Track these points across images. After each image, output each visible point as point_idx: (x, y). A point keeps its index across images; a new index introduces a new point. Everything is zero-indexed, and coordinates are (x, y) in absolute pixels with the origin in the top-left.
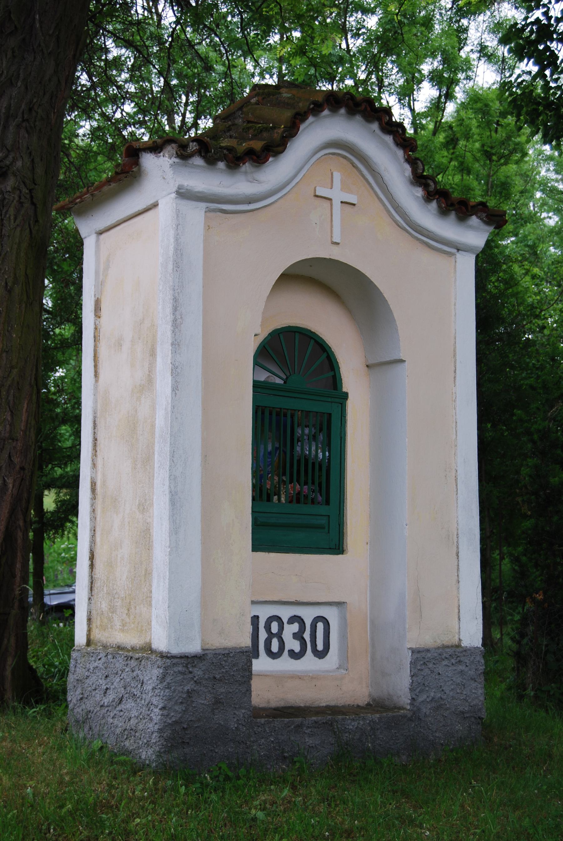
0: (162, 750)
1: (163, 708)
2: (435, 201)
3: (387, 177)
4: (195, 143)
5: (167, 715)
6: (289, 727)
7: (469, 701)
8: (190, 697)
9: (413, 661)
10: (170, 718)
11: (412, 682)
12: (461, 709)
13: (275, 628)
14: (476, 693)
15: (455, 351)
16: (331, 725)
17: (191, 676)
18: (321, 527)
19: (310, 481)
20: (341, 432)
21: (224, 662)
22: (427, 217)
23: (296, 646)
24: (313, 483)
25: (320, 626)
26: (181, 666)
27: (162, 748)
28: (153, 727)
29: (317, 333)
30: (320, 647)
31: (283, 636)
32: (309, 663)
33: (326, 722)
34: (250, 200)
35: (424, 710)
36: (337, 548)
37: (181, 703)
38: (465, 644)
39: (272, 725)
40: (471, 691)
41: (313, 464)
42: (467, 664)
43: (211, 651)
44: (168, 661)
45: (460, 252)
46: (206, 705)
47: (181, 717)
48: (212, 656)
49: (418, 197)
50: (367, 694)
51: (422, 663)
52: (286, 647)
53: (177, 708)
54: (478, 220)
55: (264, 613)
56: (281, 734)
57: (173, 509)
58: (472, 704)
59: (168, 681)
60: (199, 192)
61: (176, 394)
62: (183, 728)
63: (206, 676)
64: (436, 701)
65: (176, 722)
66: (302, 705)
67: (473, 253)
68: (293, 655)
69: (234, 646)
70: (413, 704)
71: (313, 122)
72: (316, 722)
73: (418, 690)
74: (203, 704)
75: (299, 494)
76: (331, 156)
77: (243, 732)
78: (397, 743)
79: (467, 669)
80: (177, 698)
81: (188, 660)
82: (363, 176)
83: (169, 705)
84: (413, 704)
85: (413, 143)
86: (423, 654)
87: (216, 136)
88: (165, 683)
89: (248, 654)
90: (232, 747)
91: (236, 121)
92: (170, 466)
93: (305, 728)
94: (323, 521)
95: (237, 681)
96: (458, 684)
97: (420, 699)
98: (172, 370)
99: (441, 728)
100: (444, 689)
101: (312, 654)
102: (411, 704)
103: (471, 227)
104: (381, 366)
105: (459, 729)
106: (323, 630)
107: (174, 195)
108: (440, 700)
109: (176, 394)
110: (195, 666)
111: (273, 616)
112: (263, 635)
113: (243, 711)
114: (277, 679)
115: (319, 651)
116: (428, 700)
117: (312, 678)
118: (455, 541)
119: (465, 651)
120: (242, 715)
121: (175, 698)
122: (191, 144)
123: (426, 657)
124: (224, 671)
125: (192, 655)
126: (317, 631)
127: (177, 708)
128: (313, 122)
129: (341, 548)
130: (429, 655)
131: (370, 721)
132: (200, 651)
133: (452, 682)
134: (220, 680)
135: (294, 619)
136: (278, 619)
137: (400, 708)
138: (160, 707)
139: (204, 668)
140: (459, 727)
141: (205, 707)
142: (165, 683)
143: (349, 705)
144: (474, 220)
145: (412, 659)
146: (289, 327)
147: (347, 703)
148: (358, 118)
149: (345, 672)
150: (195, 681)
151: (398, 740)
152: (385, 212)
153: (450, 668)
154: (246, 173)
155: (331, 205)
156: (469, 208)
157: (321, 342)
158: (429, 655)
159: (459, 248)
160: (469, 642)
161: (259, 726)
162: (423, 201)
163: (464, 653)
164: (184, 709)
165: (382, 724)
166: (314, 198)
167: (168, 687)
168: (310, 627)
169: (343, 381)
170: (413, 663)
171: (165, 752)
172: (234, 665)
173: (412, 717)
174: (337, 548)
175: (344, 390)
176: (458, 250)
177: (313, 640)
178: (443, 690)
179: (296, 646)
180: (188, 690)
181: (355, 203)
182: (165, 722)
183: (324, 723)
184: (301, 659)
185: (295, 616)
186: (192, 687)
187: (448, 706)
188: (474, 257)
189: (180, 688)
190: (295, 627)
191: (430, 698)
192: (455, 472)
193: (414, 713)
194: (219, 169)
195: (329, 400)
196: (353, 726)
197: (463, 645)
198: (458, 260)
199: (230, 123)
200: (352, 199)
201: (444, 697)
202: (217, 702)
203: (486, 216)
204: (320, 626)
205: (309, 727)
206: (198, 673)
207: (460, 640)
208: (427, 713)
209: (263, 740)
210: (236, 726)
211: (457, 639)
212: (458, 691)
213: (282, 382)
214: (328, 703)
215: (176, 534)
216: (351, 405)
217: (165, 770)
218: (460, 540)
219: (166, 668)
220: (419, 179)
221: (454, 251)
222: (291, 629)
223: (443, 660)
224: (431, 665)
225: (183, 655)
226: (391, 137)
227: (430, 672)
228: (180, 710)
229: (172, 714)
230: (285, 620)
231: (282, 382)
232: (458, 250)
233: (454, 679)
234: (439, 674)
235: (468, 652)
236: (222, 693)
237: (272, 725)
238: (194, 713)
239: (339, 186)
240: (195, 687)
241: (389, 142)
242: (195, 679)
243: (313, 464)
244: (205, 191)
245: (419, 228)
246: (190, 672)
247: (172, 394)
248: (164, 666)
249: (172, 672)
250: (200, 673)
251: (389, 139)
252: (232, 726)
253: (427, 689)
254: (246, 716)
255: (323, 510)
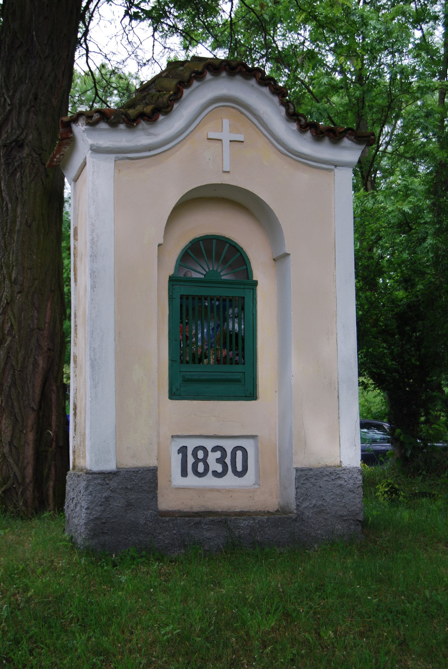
0: (87, 538)
1: (87, 509)
2: (309, 132)
3: (265, 118)
4: (97, 114)
5: (90, 514)
6: (189, 523)
7: (348, 507)
8: (108, 501)
9: (297, 477)
10: (93, 516)
11: (297, 492)
12: (340, 513)
13: (201, 455)
14: (356, 501)
15: (335, 243)
16: (226, 522)
17: (108, 486)
18: (238, 381)
19: (234, 347)
20: (253, 310)
21: (134, 477)
22: (304, 145)
23: (219, 468)
24: (237, 349)
25: (239, 454)
26: (100, 479)
27: (87, 536)
28: (82, 522)
29: (231, 238)
30: (239, 468)
31: (207, 461)
32: (230, 480)
33: (221, 521)
34: (149, 148)
35: (307, 514)
36: (251, 394)
37: (101, 505)
38: (344, 464)
39: (175, 522)
40: (349, 500)
41: (231, 336)
42: (346, 480)
43: (124, 470)
44: (90, 476)
45: (337, 167)
46: (120, 507)
47: (101, 515)
48: (124, 473)
49: (294, 130)
50: (277, 503)
51: (304, 478)
52: (210, 469)
53: (97, 508)
54: (350, 142)
55: (191, 444)
56: (183, 529)
57: (93, 371)
58: (350, 510)
59: (90, 490)
60: (106, 147)
61: (94, 290)
62: (103, 522)
63: (120, 487)
64: (317, 507)
65: (97, 518)
66: (220, 510)
67: (351, 167)
68: (215, 474)
69: (144, 466)
70: (298, 509)
71: (198, 86)
72: (212, 521)
73: (302, 499)
74: (118, 506)
75: (225, 357)
76: (221, 108)
77: (150, 527)
78: (283, 538)
79: (345, 483)
80: (97, 502)
81: (106, 476)
82: (250, 119)
83: (92, 507)
84: (298, 509)
85: (283, 91)
86: (306, 472)
87: (134, 104)
88: (88, 491)
89: (153, 471)
90: (142, 537)
91: (150, 92)
92: (90, 341)
93: (203, 525)
94: (237, 376)
95: (145, 490)
96: (337, 495)
97: (304, 506)
98: (91, 274)
99: (323, 528)
100: (325, 498)
101: (232, 474)
102: (297, 509)
103: (345, 148)
104: (280, 259)
105: (339, 529)
106: (241, 457)
107: (90, 152)
108: (321, 506)
109: (94, 290)
110: (111, 480)
111: (201, 446)
112: (191, 460)
113: (151, 512)
114: (180, 490)
115: (238, 472)
116: (310, 506)
117: (229, 491)
118: (337, 387)
119: (344, 470)
120: (149, 515)
121: (95, 501)
122: (95, 115)
123: (309, 474)
124: (134, 483)
125: (108, 472)
126: (237, 457)
127: (97, 508)
128: (198, 86)
129: (255, 396)
130: (311, 473)
131: (259, 521)
132: (115, 469)
133: (332, 493)
134: (131, 489)
135: (215, 449)
136: (204, 449)
137: (291, 513)
138: (85, 507)
139: (118, 481)
140: (339, 527)
141: (119, 508)
142: (88, 491)
143: (260, 511)
144: (346, 142)
145: (296, 476)
146: (207, 235)
147: (259, 510)
148: (238, 77)
149: (258, 487)
150: (111, 490)
151: (285, 535)
152: (270, 144)
153: (330, 483)
154: (143, 129)
155: (222, 144)
156: (337, 134)
157: (234, 245)
158: (311, 473)
159: (337, 165)
160: (349, 463)
161: (164, 523)
162: (299, 133)
163: (343, 471)
164: (103, 509)
165: (269, 523)
166: (207, 140)
167: (91, 494)
168: (230, 454)
169: (253, 273)
170: (298, 479)
171: (89, 539)
172: (142, 479)
173: (296, 518)
174: (251, 394)
175: (255, 279)
176: (336, 166)
177: (233, 462)
178: (324, 499)
179: (219, 468)
180: (106, 496)
181: (242, 140)
182: (88, 518)
183: (219, 521)
184: (223, 478)
185: (217, 446)
186: (109, 494)
187: (328, 511)
188: (352, 169)
189: (100, 495)
190: (218, 454)
191: (313, 505)
192: (336, 335)
193: (298, 516)
194: (121, 129)
195: (242, 287)
196: (244, 524)
197: (343, 466)
198: (336, 174)
199: (145, 93)
200: (240, 137)
201: (325, 504)
202: (129, 505)
203: (355, 138)
204: (239, 454)
205: (206, 524)
206: (113, 484)
207: (341, 462)
208: (310, 516)
209: (167, 533)
210: (144, 522)
211: (339, 462)
212: (338, 500)
213: (203, 277)
214: (242, 510)
215: (95, 388)
216: (260, 291)
217: (89, 552)
218: (340, 386)
219: (89, 481)
220: (292, 116)
221: (332, 167)
222: (213, 457)
223: (324, 476)
224: (313, 480)
225: (100, 472)
226: (268, 88)
227: (312, 486)
228: (100, 510)
229: (94, 513)
230: (209, 449)
231: (203, 277)
232: (336, 166)
233: (334, 491)
234: (321, 487)
235: (347, 470)
236: (133, 498)
237: (175, 522)
238: (110, 512)
239: (225, 129)
240: (111, 494)
241: (265, 92)
242: (111, 489)
243: (231, 336)
244: (111, 146)
245: (297, 153)
246: (107, 484)
247: (91, 290)
248: (87, 479)
249: (93, 484)
250: (115, 484)
251: (266, 90)
252: (141, 522)
253: (310, 498)
254: (153, 515)
255: (239, 368)
